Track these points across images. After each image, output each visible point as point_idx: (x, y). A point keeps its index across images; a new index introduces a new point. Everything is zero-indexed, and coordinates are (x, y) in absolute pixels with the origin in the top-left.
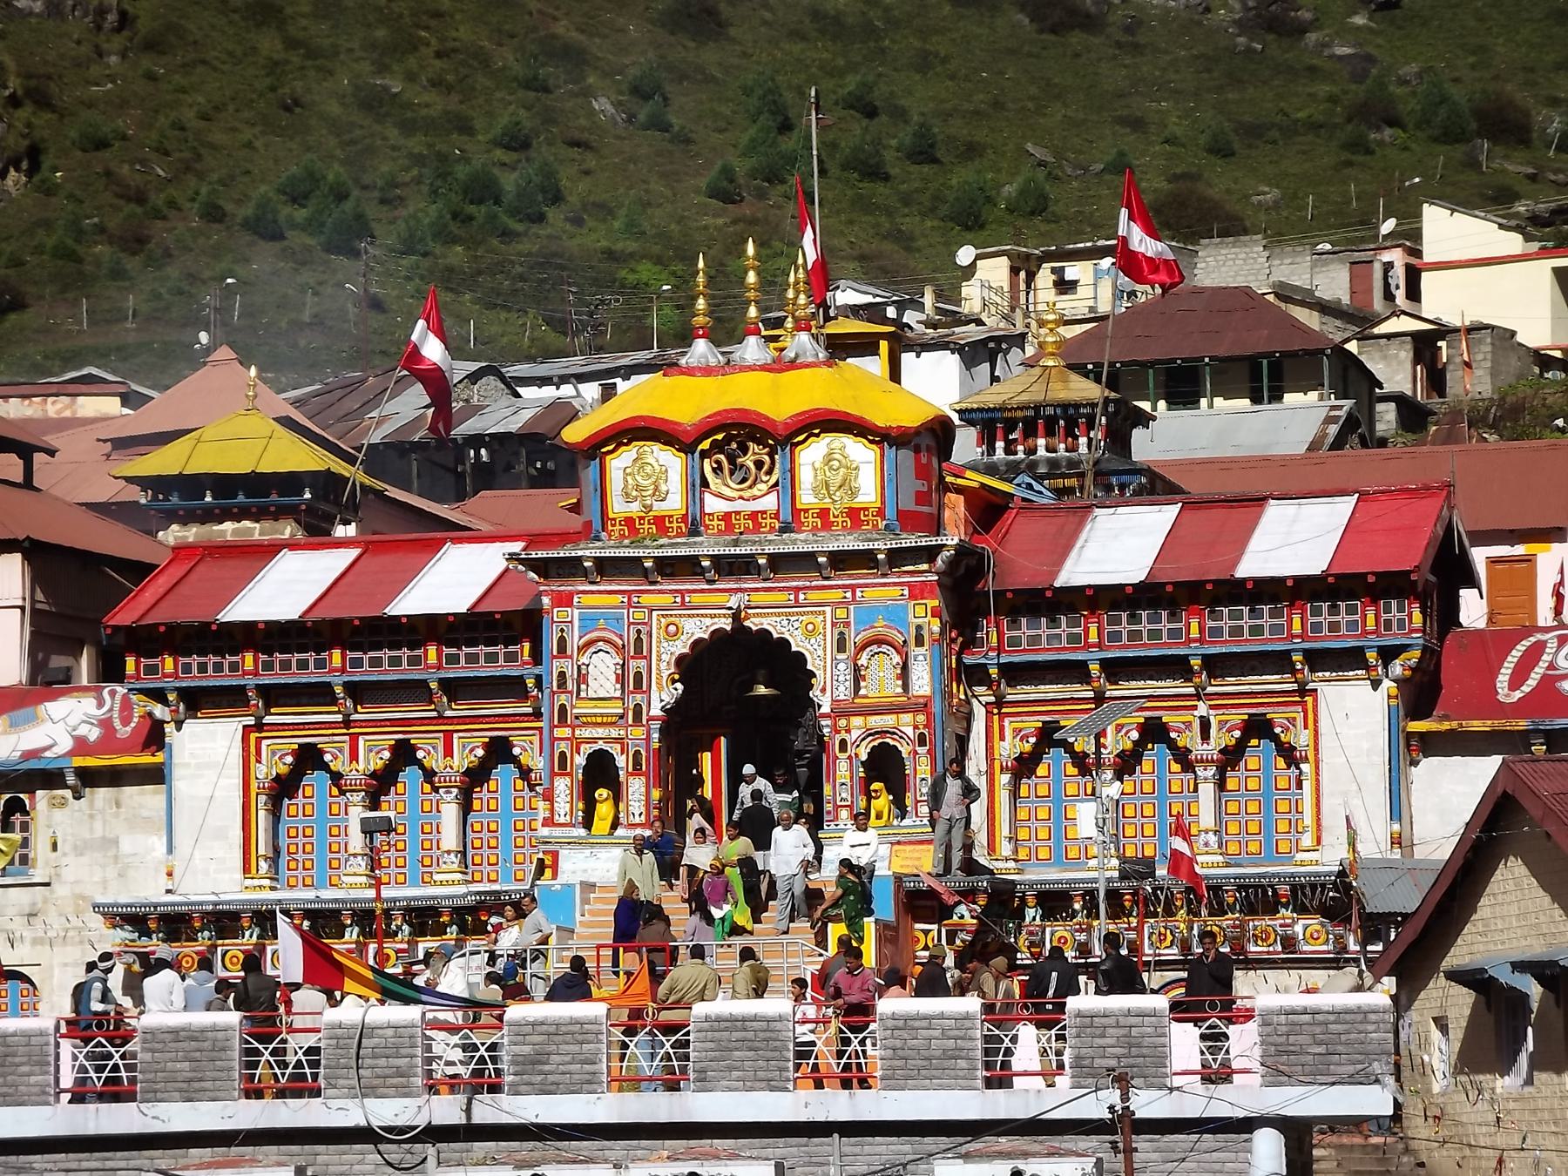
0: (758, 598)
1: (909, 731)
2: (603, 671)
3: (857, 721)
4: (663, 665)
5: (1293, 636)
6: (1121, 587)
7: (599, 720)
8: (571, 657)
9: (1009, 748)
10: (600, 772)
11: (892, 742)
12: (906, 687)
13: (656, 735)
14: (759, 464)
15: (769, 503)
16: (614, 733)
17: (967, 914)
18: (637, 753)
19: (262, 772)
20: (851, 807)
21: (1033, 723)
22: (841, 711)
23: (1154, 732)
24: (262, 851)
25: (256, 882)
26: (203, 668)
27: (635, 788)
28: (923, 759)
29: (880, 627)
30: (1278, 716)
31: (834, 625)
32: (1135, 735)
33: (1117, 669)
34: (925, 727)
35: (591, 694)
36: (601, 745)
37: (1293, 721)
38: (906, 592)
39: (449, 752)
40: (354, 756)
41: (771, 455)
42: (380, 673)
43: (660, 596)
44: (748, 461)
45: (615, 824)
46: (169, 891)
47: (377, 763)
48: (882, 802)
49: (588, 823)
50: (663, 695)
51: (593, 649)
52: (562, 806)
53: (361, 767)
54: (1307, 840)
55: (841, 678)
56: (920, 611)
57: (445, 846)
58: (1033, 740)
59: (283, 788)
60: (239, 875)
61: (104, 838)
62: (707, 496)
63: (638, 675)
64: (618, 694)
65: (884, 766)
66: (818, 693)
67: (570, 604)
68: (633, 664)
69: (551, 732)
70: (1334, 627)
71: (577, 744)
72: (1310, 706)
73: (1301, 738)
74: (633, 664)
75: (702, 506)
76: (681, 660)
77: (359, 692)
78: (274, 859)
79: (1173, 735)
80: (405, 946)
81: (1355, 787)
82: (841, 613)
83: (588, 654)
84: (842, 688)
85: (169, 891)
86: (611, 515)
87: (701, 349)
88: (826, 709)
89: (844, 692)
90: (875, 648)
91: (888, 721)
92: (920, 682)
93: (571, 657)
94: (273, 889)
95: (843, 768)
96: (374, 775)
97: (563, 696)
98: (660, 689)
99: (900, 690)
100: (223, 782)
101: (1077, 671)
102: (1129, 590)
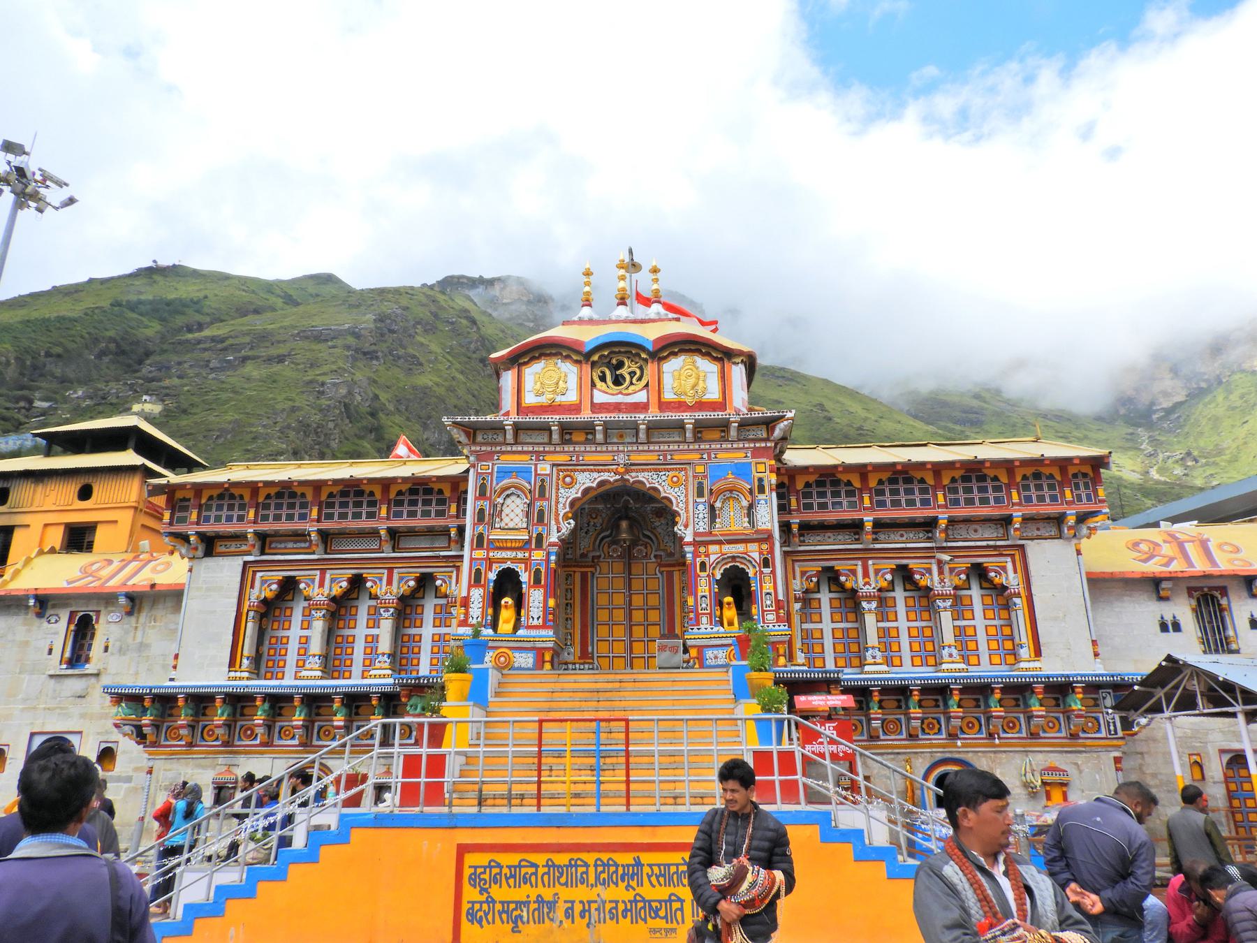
0: (636, 458)
1: (756, 556)
3: (713, 548)
4: (560, 506)
5: (1014, 504)
6: (894, 464)
9: (797, 585)
10: (507, 584)
12: (752, 522)
13: (553, 558)
14: (632, 374)
15: (641, 397)
16: (520, 555)
18: (538, 572)
20: (710, 614)
21: (814, 567)
23: (905, 575)
24: (246, 653)
25: (238, 674)
27: (535, 598)
32: (889, 577)
35: (503, 525)
36: (509, 565)
37: (1004, 568)
39: (390, 582)
40: (321, 585)
41: (641, 368)
44: (624, 371)
45: (516, 627)
46: (172, 680)
47: (336, 591)
48: (730, 613)
49: (494, 625)
50: (558, 529)
52: (476, 611)
53: (326, 592)
54: (1024, 653)
55: (701, 516)
58: (815, 579)
61: (141, 643)
64: (525, 525)
68: (538, 504)
70: (1041, 499)
71: (490, 562)
72: (1017, 557)
73: (1012, 579)
74: (538, 504)
77: (325, 536)
78: (257, 660)
79: (917, 577)
80: (342, 724)
82: (700, 469)
83: (503, 496)
84: (701, 523)
88: (689, 538)
89: (703, 527)
91: (740, 548)
93: (490, 498)
95: (703, 587)
96: (333, 599)
98: (557, 522)
99: (746, 524)
101: (857, 526)
102: (899, 467)
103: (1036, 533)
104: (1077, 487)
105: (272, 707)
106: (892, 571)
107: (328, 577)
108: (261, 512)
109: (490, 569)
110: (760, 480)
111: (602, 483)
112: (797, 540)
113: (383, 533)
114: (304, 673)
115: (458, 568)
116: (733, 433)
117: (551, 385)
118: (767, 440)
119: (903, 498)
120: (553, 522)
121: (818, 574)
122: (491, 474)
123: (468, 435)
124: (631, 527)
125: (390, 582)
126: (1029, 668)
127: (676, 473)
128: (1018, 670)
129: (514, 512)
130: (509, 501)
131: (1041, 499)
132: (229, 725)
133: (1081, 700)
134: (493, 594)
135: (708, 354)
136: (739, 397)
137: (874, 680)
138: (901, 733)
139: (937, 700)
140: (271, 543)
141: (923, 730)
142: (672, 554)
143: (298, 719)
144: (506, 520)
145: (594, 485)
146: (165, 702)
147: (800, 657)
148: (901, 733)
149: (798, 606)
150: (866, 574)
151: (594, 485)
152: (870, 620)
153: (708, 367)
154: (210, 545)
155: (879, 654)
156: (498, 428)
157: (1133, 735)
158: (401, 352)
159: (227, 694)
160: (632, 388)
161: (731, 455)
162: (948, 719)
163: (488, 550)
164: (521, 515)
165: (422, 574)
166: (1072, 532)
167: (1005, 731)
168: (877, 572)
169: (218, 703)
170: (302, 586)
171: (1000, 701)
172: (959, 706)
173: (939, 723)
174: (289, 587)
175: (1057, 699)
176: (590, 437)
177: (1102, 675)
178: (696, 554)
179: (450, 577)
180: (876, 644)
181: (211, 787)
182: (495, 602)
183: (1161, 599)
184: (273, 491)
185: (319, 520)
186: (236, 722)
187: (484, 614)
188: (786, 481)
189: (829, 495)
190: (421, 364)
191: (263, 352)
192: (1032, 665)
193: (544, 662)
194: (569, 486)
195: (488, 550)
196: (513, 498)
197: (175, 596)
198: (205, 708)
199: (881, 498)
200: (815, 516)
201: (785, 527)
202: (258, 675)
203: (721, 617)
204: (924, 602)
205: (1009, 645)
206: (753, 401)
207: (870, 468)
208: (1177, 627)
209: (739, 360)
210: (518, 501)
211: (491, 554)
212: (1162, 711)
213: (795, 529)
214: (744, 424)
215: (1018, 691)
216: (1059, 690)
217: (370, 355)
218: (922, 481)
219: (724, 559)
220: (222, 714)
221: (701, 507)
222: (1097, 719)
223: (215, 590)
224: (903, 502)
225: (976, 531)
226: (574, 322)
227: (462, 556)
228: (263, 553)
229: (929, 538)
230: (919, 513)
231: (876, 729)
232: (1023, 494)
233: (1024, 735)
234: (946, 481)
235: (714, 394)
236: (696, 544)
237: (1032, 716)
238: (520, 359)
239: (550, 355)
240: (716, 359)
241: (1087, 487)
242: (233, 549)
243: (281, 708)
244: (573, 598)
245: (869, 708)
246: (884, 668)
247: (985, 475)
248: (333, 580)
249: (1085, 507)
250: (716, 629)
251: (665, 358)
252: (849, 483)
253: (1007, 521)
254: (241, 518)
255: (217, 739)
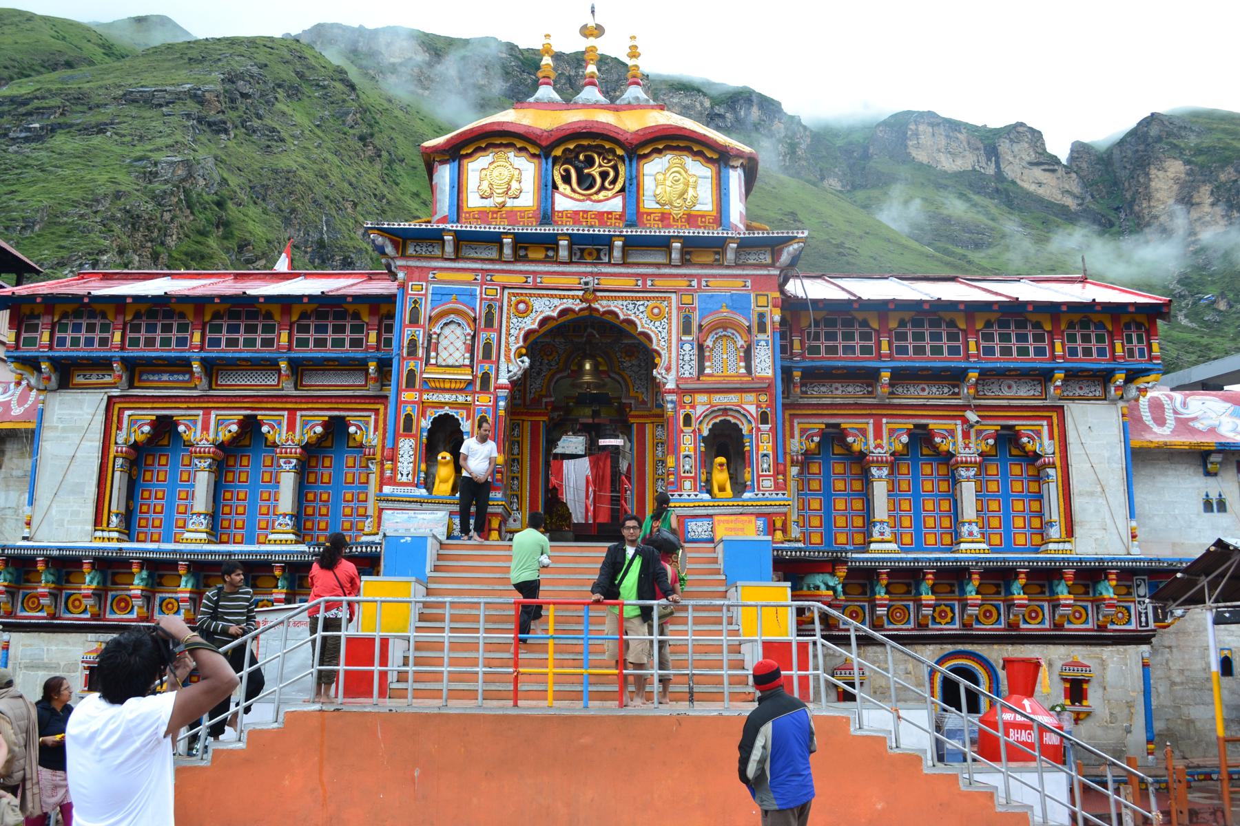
0: (607, 283)
1: (752, 409)
3: (701, 398)
6: (921, 302)
7: (447, 386)
8: (423, 327)
9: (796, 445)
11: (733, 421)
12: (748, 368)
13: (502, 404)
14: (604, 175)
15: (616, 204)
16: (461, 399)
17: (823, 587)
19: (121, 437)
20: (694, 478)
21: (817, 425)
23: (921, 438)
24: (114, 508)
25: (106, 534)
26: (75, 342)
28: (765, 437)
29: (725, 313)
30: (1022, 425)
31: (679, 309)
32: (905, 439)
33: (902, 376)
34: (768, 406)
35: (440, 361)
36: (447, 410)
37: (1038, 433)
38: (749, 284)
40: (206, 428)
41: (615, 168)
42: (234, 352)
43: (513, 275)
44: (595, 171)
46: (25, 538)
47: (224, 436)
48: (721, 477)
49: (428, 484)
50: (510, 367)
51: (444, 321)
52: (406, 464)
53: (211, 438)
54: (1054, 532)
55: (687, 358)
56: (763, 301)
57: (281, 510)
58: (816, 439)
59: (140, 458)
60: (90, 527)
62: (557, 196)
63: (488, 347)
64: (467, 362)
65: (726, 442)
66: (663, 371)
67: (427, 282)
68: (483, 336)
69: (398, 395)
70: (1087, 352)
71: (424, 407)
73: (1047, 446)
75: (553, 203)
76: (528, 334)
78: (128, 518)
79: (938, 440)
81: (1099, 489)
84: (687, 367)
85: (25, 538)
86: (465, 209)
87: (546, 92)
88: (671, 385)
89: (689, 370)
90: (721, 332)
91: (733, 399)
92: (764, 365)
93: (423, 327)
94: (119, 540)
96: (221, 446)
97: (412, 364)
99: (743, 371)
100: (86, 444)
101: (869, 377)
102: (926, 307)
103: (1078, 392)
104: (1130, 341)
105: (149, 576)
106: (910, 433)
107: (213, 416)
108: (130, 335)
109: (424, 415)
110: (761, 316)
111: (563, 313)
112: (798, 390)
113: (283, 365)
114: (187, 535)
115: (377, 411)
116: (730, 255)
117: (502, 185)
118: (772, 265)
119: (928, 344)
120: (502, 359)
121: (822, 434)
122: (425, 295)
123: (396, 245)
124: (595, 366)
125: (291, 427)
126: (1056, 550)
127: (658, 303)
128: (1046, 551)
129: (453, 346)
130: (447, 331)
131: (1087, 352)
132: (99, 595)
133: (1115, 587)
134: (427, 445)
135: (699, 154)
136: (736, 209)
137: (884, 560)
138: (908, 622)
139: (952, 585)
140: (140, 376)
141: (934, 618)
142: (644, 402)
143: (185, 586)
144: (444, 354)
145: (555, 314)
147: (795, 532)
148: (908, 622)
149: (794, 470)
150: (878, 435)
151: (555, 314)
152: (880, 490)
153: (699, 171)
154: (66, 374)
155: (887, 530)
156: (435, 237)
157: (1165, 627)
158: (256, 123)
159: (95, 558)
160: (603, 193)
161: (722, 286)
162: (964, 607)
163: (421, 392)
164: (462, 348)
165: (330, 417)
166: (1120, 393)
167: (1026, 622)
168: (892, 432)
169: (86, 568)
170: (181, 428)
171: (1024, 587)
172: (977, 593)
173: (953, 611)
174: (164, 429)
175: (1086, 586)
176: (551, 253)
177: (1140, 560)
178: (680, 404)
179: (367, 423)
180: (885, 518)
181: (81, 665)
182: (429, 452)
183: (1208, 474)
184: (143, 308)
185: (202, 348)
186: (106, 591)
187: (416, 471)
188: (789, 318)
189: (840, 337)
190: (282, 140)
191: (77, 119)
192: (1061, 546)
193: (490, 530)
194: (523, 314)
195: (421, 392)
196: (453, 327)
198: (69, 574)
199: (902, 343)
200: (823, 360)
201: (787, 373)
202: (128, 535)
203: (709, 481)
204: (943, 470)
205: (1036, 523)
206: (750, 218)
207: (891, 306)
208: (1222, 506)
209: (738, 163)
210: (458, 331)
211: (425, 397)
212: (1204, 602)
213: (797, 375)
214: (745, 245)
215: (1044, 577)
216: (1090, 575)
217: (218, 128)
218: (952, 324)
219: (713, 412)
220: (91, 582)
221: (687, 347)
222: (1128, 609)
223: (75, 427)
224: (928, 349)
225: (1010, 387)
226: (530, 106)
227: (386, 397)
228: (131, 386)
229: (954, 394)
230: (945, 361)
231: (880, 617)
232: (1068, 345)
233: (1047, 625)
234: (979, 326)
235: (705, 202)
236: (680, 391)
237: (1059, 605)
238: (458, 151)
239: (501, 145)
240: (710, 160)
241: (1140, 340)
242: (94, 380)
243: (161, 577)
244: (521, 453)
245: (873, 593)
246: (894, 546)
247: (1027, 320)
248: (219, 423)
249: (1138, 363)
250: (700, 496)
251: (645, 156)
252: (865, 323)
253: (1044, 377)
254: (103, 342)
255: (85, 611)
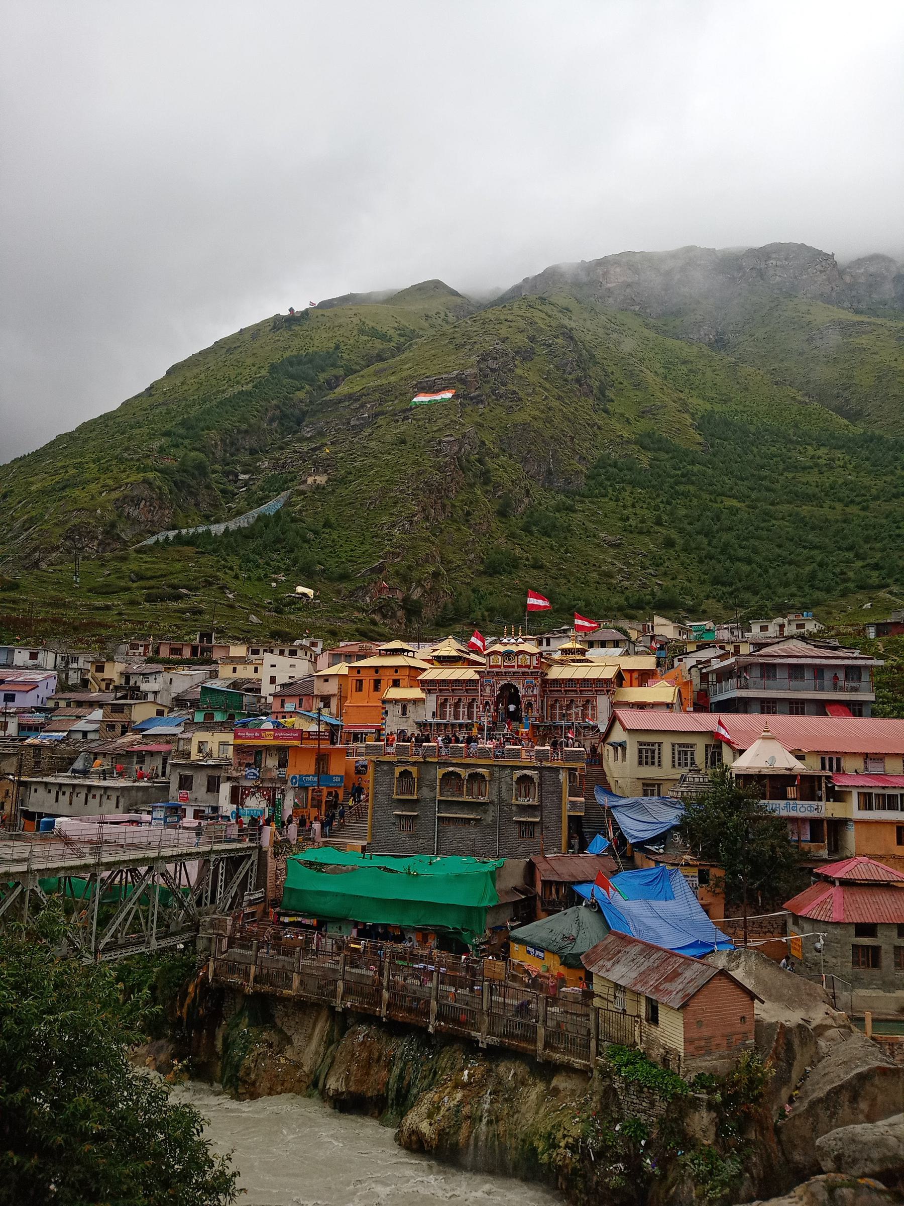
2: (488, 689)
22: (523, 696)
129: (488, 689)
146: (425, 725)
154: (429, 692)
182: (484, 707)
197: (423, 701)
